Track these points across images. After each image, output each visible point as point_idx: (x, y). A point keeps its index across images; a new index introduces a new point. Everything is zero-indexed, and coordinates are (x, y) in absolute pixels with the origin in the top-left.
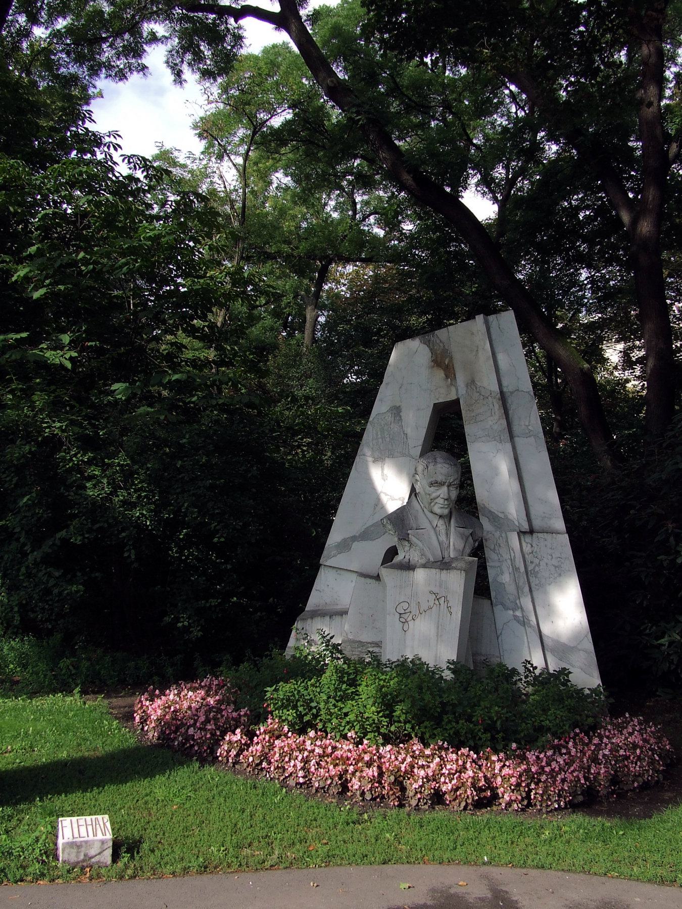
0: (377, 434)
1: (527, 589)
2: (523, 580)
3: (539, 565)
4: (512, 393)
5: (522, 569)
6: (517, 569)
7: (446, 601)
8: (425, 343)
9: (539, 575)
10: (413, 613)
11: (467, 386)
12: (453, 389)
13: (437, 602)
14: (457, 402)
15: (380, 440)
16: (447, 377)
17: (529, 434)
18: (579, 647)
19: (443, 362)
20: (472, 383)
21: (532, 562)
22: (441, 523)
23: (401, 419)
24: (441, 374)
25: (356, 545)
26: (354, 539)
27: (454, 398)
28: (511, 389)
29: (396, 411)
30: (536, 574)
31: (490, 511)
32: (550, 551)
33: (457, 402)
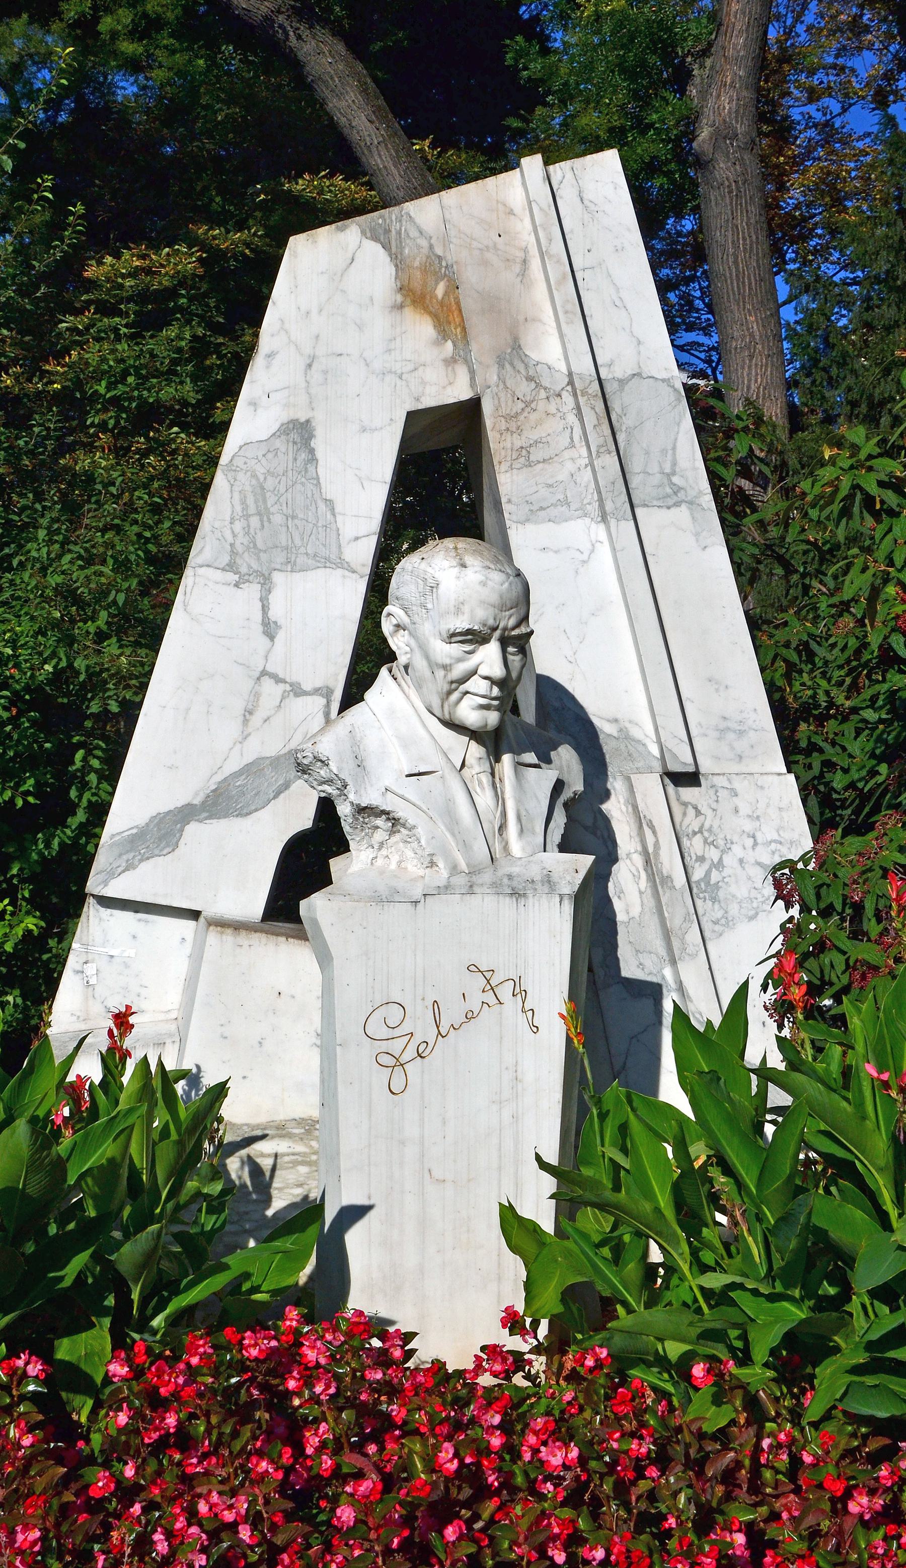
0: (243, 502)
1: (694, 935)
2: (678, 912)
3: (719, 865)
4: (622, 382)
5: (680, 879)
6: (667, 880)
7: (520, 992)
8: (375, 238)
9: (721, 894)
11: (501, 365)
13: (490, 998)
14: (471, 409)
15: (255, 521)
16: (443, 333)
17: (673, 497)
19: (431, 294)
20: (513, 353)
21: (701, 859)
22: (476, 750)
23: (312, 459)
24: (422, 328)
25: (192, 830)
26: (186, 814)
27: (465, 394)
28: (620, 370)
29: (300, 433)
30: (713, 890)
32: (748, 826)
33: (471, 409)
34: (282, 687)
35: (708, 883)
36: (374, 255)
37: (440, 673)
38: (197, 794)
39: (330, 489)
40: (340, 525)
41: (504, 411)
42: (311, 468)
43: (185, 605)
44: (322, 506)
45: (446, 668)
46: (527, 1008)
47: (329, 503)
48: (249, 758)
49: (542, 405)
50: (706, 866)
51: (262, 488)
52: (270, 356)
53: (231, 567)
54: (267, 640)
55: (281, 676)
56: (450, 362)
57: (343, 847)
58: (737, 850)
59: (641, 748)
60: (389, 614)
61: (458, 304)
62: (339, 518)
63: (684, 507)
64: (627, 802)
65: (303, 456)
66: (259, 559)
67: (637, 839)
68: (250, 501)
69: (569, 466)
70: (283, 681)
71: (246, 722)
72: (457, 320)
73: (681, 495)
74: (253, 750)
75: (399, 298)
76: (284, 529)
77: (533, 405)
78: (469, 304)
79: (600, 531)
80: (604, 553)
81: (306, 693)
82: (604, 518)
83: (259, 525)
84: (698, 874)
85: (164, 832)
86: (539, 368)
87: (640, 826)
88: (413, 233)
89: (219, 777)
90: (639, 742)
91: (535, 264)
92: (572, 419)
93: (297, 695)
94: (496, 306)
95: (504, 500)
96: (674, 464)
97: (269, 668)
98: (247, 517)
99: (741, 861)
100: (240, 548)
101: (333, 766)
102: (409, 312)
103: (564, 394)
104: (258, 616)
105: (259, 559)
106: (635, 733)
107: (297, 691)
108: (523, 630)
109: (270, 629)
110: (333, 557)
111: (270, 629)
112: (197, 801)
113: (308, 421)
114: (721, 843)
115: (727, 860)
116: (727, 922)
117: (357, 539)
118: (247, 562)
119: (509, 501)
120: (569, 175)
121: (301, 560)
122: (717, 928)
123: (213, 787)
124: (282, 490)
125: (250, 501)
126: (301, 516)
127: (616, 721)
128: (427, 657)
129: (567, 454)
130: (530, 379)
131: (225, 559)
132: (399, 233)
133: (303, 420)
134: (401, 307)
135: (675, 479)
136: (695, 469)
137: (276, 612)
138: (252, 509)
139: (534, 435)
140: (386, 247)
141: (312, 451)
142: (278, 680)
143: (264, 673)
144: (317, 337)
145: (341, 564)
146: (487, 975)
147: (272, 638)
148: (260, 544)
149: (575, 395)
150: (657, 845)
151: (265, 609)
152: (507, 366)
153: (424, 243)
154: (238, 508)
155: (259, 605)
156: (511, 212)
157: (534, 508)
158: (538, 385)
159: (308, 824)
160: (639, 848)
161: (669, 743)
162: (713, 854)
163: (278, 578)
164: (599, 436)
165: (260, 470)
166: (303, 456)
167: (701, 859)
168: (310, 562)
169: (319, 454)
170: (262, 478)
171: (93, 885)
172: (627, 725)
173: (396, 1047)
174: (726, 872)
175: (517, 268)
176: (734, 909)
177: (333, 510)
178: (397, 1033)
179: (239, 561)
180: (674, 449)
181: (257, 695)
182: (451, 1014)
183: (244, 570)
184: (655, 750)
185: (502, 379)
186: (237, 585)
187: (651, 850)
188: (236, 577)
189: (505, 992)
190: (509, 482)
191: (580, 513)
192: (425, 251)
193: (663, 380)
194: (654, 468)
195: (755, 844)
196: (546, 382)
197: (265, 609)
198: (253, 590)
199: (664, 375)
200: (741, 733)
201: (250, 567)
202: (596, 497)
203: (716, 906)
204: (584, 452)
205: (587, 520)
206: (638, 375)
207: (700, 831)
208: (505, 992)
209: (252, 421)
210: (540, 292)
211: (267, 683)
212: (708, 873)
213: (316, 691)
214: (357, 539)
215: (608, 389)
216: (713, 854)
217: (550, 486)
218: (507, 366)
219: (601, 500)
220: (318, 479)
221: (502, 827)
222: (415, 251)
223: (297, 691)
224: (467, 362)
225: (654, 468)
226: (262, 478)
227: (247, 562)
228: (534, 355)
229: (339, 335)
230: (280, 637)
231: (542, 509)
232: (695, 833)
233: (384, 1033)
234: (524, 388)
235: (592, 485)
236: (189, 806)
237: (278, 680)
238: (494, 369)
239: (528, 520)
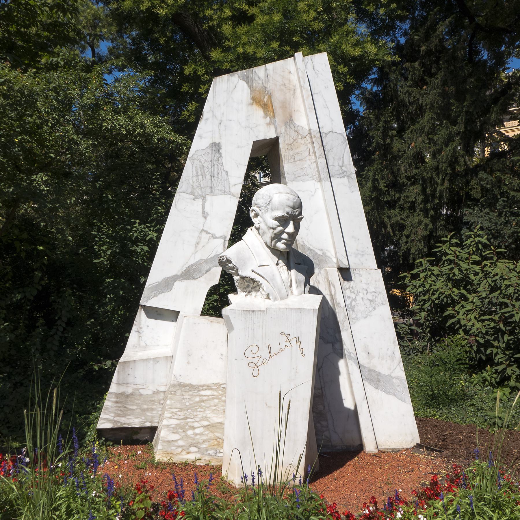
3: (355, 299)
5: (343, 304)
7: (298, 341)
9: (356, 309)
10: (263, 358)
12: (272, 127)
13: (288, 344)
15: (200, 178)
16: (266, 115)
18: (393, 375)
19: (262, 101)
21: (349, 297)
24: (260, 112)
25: (177, 284)
26: (175, 278)
27: (274, 136)
29: (216, 147)
30: (353, 308)
31: (309, 249)
32: (365, 287)
34: (209, 235)
35: (351, 306)
36: (243, 85)
37: (272, 230)
38: (179, 271)
39: (227, 167)
40: (230, 180)
41: (287, 142)
42: (220, 159)
43: (176, 205)
44: (224, 173)
45: (274, 229)
46: (301, 347)
48: (197, 259)
49: (300, 141)
50: (350, 300)
51: (203, 166)
52: (206, 119)
53: (192, 193)
54: (204, 219)
55: (209, 231)
56: (269, 124)
58: (361, 295)
59: (330, 259)
60: (253, 210)
61: (272, 103)
62: (229, 177)
63: (346, 177)
64: (325, 278)
65: (217, 155)
66: (201, 191)
67: (328, 290)
68: (199, 170)
69: (308, 162)
70: (209, 233)
71: (196, 247)
72: (271, 110)
73: (345, 174)
74: (198, 257)
75: (251, 101)
76: (210, 181)
77: (297, 141)
78: (276, 105)
79: (318, 185)
80: (320, 193)
81: (217, 238)
82: (320, 180)
83: (202, 179)
84: (348, 302)
85: (167, 284)
86: (299, 128)
87: (330, 286)
88: (257, 78)
89: (187, 266)
90: (329, 257)
91: (298, 91)
92: (310, 146)
93: (214, 238)
94: (285, 106)
95: (286, 173)
96: (343, 163)
97: (205, 229)
98: (198, 176)
99: (362, 298)
100: (195, 187)
101: (233, 262)
102: (255, 106)
103: (307, 137)
104: (201, 210)
105: (201, 191)
106: (328, 254)
107: (214, 237)
108: (301, 217)
109: (205, 215)
110: (227, 191)
111: (205, 215)
112: (179, 274)
113: (219, 143)
114: (356, 292)
115: (358, 298)
116: (357, 318)
117: (235, 185)
118: (198, 191)
119: (288, 174)
120: (310, 61)
121: (216, 192)
122: (354, 321)
123: (185, 269)
124: (210, 167)
125: (199, 170)
126: (216, 176)
127: (322, 250)
128: (266, 225)
129: (308, 158)
130: (296, 131)
131: (190, 190)
132: (252, 78)
133: (217, 143)
134: (252, 104)
135: (343, 168)
136: (350, 165)
138: (200, 174)
139: (297, 151)
140: (247, 83)
141: (220, 154)
142: (208, 233)
144: (223, 114)
145: (230, 193)
146: (288, 336)
147: (206, 218)
148: (202, 186)
149: (311, 137)
150: (335, 291)
151: (203, 208)
152: (288, 127)
153: (260, 82)
154: (195, 172)
155: (201, 206)
156: (290, 72)
157: (296, 176)
158: (298, 134)
159: (218, 283)
160: (329, 293)
161: (341, 258)
162: (353, 296)
163: (208, 197)
164: (319, 151)
165: (203, 160)
166: (217, 155)
167: (349, 297)
168: (219, 192)
169: (223, 155)
170: (203, 162)
171: (142, 302)
172: (326, 252)
173: (255, 360)
174: (358, 302)
175: (292, 92)
176: (359, 315)
177: (227, 174)
178: (256, 355)
179: (195, 191)
180: (343, 157)
181: (200, 238)
183: (196, 194)
184: (335, 260)
185: (286, 131)
186: (194, 200)
187: (333, 294)
188: (194, 197)
189: (294, 342)
190: (287, 166)
191: (312, 178)
192: (261, 85)
193: (340, 134)
194: (336, 164)
195: (367, 293)
196: (301, 133)
197: (203, 208)
198: (199, 201)
199: (341, 132)
200: (363, 255)
201: (198, 193)
202: (317, 173)
203: (354, 313)
204: (313, 157)
205: (314, 181)
206: (332, 131)
207: (349, 288)
208: (294, 342)
209: (200, 143)
210: (299, 101)
211: (204, 234)
212: (351, 302)
213: (221, 237)
214: (235, 185)
215: (323, 135)
216: (353, 296)
217: (302, 169)
218: (288, 127)
219: (319, 174)
220: (222, 163)
221: (291, 286)
222: (258, 84)
223: (214, 237)
224: (274, 124)
225: (336, 164)
226: (203, 162)
227: (198, 191)
228: (297, 123)
229: (230, 114)
230: (208, 218)
231: (299, 177)
232: (347, 289)
233: (252, 355)
234: (294, 135)
235: (316, 169)
236: (176, 275)
237: (208, 233)
238: (283, 127)
239: (294, 180)
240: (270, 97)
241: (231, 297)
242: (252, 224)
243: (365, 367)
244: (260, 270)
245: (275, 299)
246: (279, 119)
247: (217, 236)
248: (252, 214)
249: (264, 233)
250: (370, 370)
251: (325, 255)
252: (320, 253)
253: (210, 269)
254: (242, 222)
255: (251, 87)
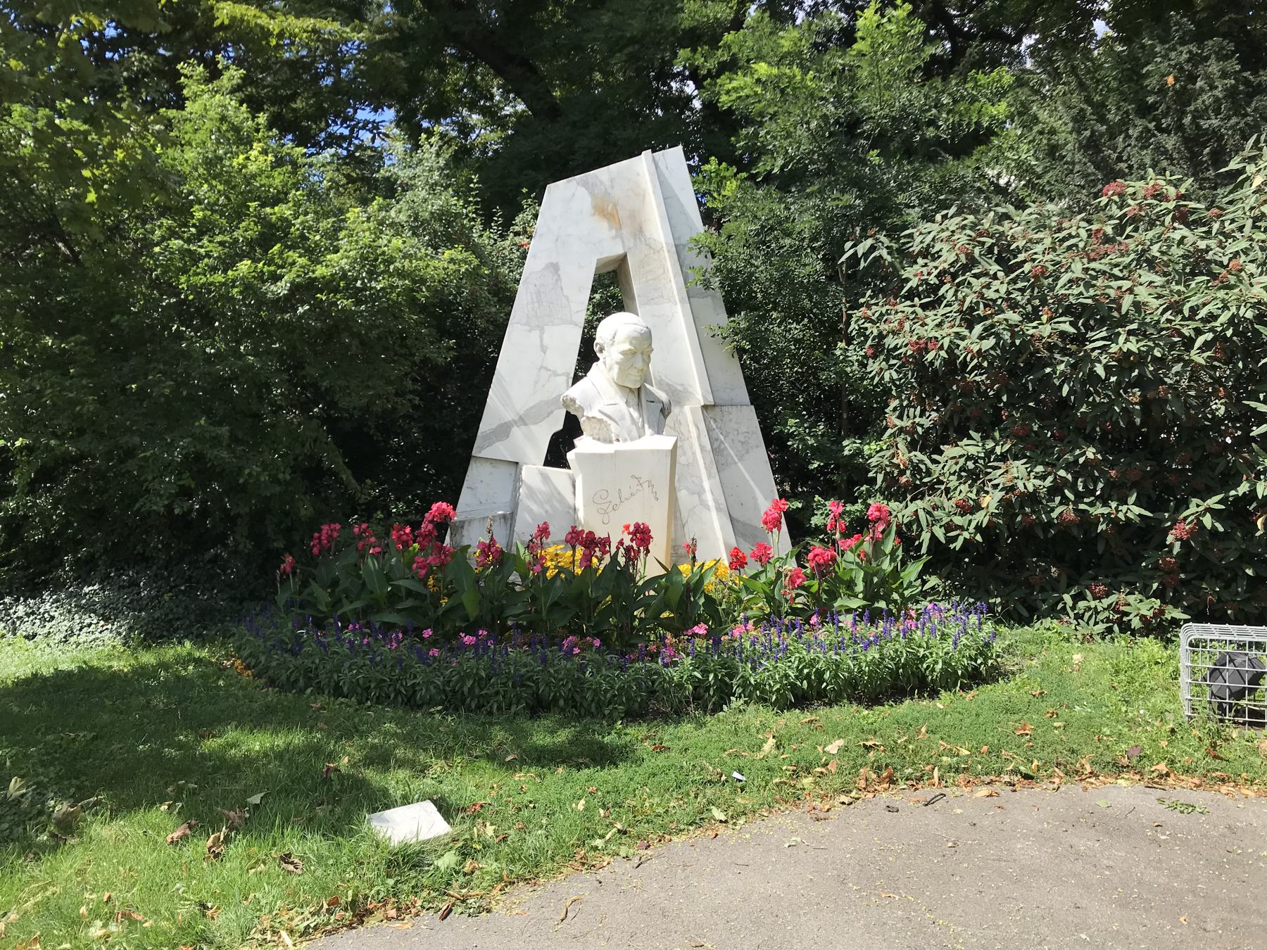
14: (623, 260)
19: (606, 210)
20: (639, 232)
23: (559, 279)
27: (619, 251)
29: (555, 267)
33: (623, 260)
36: (582, 191)
47: (567, 298)
53: (527, 324)
56: (616, 237)
57: (579, 432)
102: (596, 217)
107: (555, 374)
109: (544, 349)
111: (544, 349)
137: (546, 342)
143: (542, 367)
151: (542, 340)
173: (604, 507)
182: (625, 493)
197: (542, 340)
198: (536, 333)
211: (543, 371)
223: (555, 374)
240: (615, 205)
241: (576, 441)
242: (598, 359)
243: (738, 521)
244: (609, 410)
245: (625, 440)
246: (626, 232)
247: (559, 372)
248: (596, 349)
249: (611, 369)
250: (744, 524)
251: (686, 391)
252: (679, 388)
253: (552, 412)
254: (587, 356)
255: (592, 194)
